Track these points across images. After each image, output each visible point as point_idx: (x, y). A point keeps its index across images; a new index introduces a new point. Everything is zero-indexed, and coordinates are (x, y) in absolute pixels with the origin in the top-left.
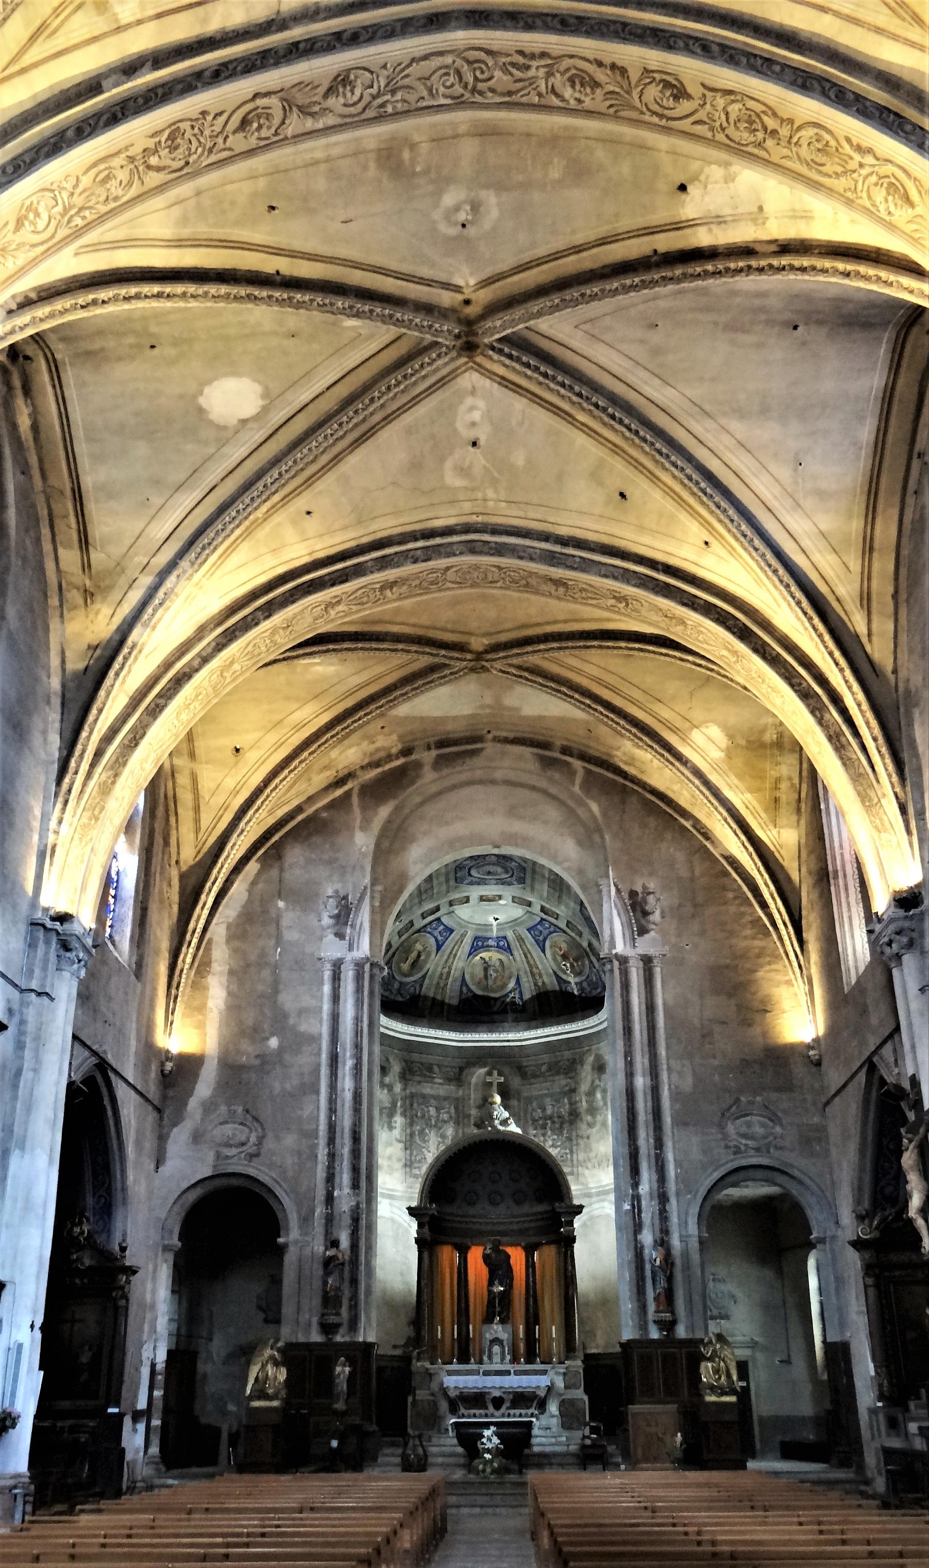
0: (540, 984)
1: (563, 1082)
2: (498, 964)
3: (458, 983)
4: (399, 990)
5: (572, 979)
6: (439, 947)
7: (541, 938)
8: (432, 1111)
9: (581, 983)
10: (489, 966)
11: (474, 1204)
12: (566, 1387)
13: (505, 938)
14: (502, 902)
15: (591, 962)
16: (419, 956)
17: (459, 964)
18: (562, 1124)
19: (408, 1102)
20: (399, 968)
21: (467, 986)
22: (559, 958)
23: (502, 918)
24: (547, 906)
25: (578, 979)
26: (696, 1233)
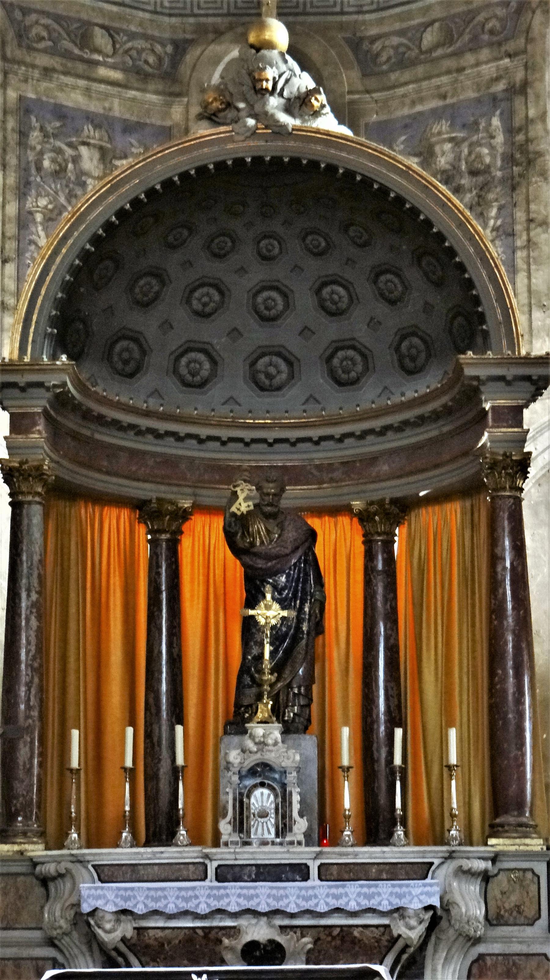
1: (488, 70)
8: (89, 160)
11: (202, 385)
12: (493, 920)
18: (484, 187)
19: (11, 123)
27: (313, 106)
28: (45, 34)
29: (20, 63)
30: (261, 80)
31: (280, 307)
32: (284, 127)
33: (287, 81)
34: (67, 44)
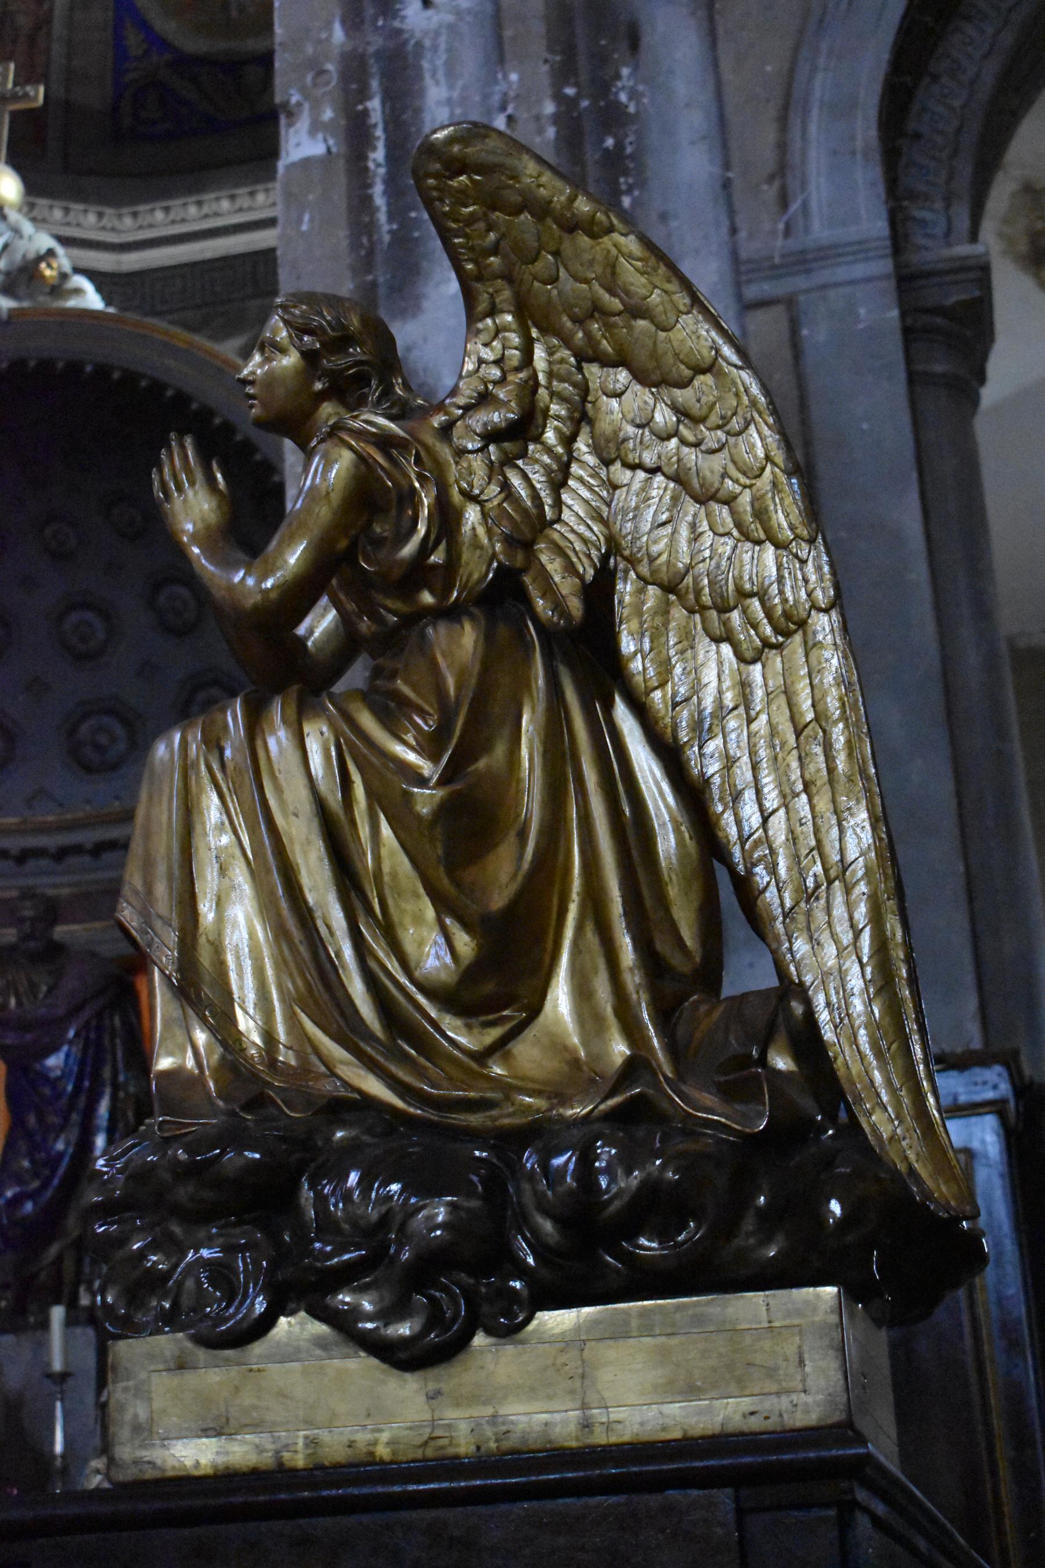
21: (144, 26)
26: (873, 224)
31: (101, 635)
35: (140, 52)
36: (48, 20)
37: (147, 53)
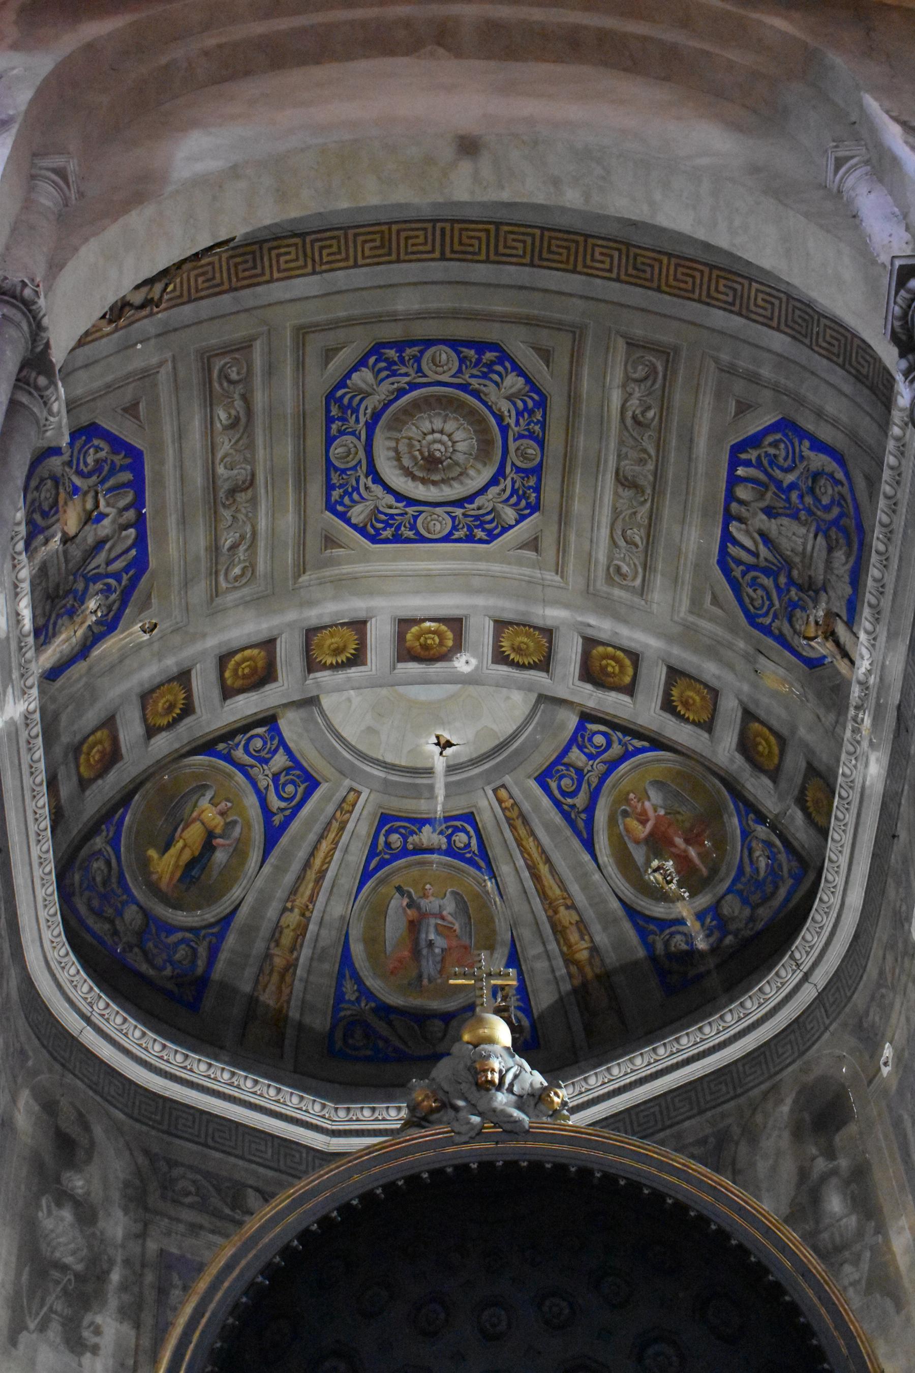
0: (583, 955)
2: (449, 907)
3: (331, 966)
4: (141, 934)
5: (685, 909)
6: (272, 836)
7: (580, 801)
9: (715, 909)
10: (424, 915)
13: (470, 818)
14: (464, 664)
15: (750, 809)
16: (208, 847)
17: (335, 904)
19: (150, 1277)
20: (144, 864)
22: (639, 854)
23: (465, 739)
24: (604, 626)
25: (704, 900)
27: (552, 1101)
28: (193, 1189)
29: (163, 1215)
30: (485, 1071)
32: (517, 1122)
33: (516, 1077)
34: (215, 1201)
35: (353, 998)
36: (296, 966)
37: (358, 1000)
